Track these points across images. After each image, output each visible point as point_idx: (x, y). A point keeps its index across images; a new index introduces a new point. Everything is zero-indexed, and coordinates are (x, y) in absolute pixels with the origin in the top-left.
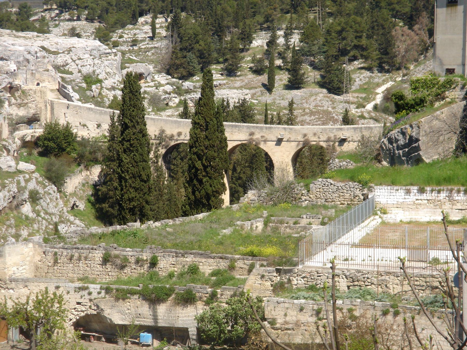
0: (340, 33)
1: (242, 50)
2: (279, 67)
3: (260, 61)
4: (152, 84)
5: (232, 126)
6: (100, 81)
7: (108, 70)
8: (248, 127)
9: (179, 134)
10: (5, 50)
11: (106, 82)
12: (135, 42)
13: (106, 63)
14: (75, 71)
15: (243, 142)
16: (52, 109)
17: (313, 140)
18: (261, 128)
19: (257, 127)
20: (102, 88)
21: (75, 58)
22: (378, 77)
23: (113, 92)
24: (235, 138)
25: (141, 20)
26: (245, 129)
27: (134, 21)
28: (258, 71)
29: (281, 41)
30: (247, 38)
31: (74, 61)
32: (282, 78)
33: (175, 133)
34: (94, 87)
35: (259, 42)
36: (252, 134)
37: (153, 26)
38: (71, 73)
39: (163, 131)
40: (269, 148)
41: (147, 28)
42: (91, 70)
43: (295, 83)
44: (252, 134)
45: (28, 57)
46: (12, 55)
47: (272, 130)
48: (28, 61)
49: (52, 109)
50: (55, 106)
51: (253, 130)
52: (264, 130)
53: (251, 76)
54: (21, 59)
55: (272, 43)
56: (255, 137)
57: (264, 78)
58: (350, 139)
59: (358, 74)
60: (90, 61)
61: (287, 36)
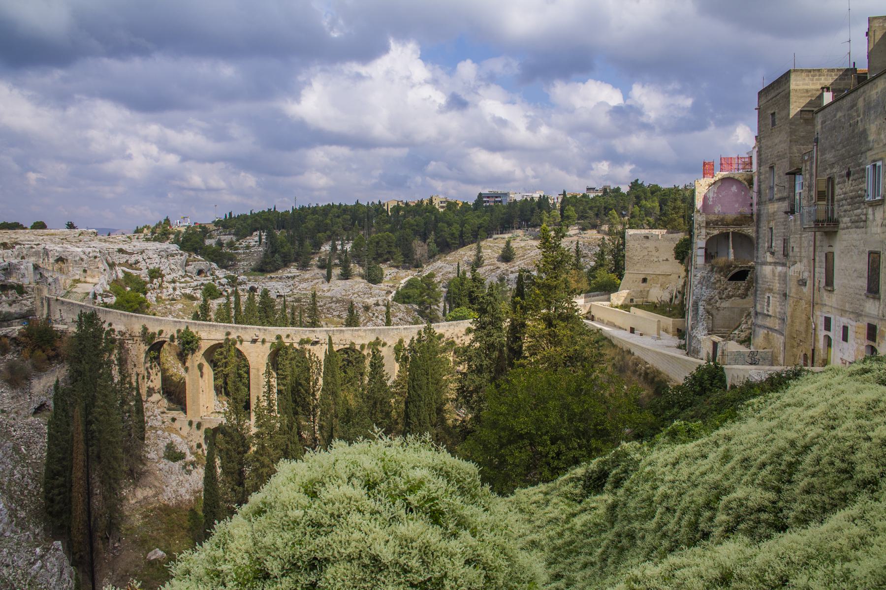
0: (378, 243)
1: (313, 253)
2: (336, 265)
3: (324, 260)
4: (211, 278)
5: (210, 325)
6: (164, 276)
7: (173, 267)
8: (225, 327)
9: (161, 332)
11: (167, 277)
12: (248, 247)
13: (172, 261)
14: (144, 268)
16: (49, 305)
17: (287, 342)
18: (237, 328)
19: (233, 327)
20: (163, 281)
21: (145, 257)
22: (402, 273)
24: (212, 337)
25: (255, 233)
26: (222, 329)
27: (251, 234)
28: (321, 267)
29: (339, 247)
30: (317, 245)
32: (337, 271)
33: (157, 331)
34: (155, 280)
35: (326, 248)
36: (228, 334)
37: (260, 236)
38: (141, 269)
39: (145, 329)
40: (246, 348)
41: (257, 239)
42: (157, 266)
43: (346, 275)
44: (228, 334)
45: (84, 257)
48: (82, 260)
49: (49, 305)
50: (52, 303)
53: (317, 271)
54: (78, 258)
55: (334, 248)
56: (230, 337)
57: (325, 272)
58: (323, 342)
59: (388, 271)
60: (158, 260)
61: (342, 245)
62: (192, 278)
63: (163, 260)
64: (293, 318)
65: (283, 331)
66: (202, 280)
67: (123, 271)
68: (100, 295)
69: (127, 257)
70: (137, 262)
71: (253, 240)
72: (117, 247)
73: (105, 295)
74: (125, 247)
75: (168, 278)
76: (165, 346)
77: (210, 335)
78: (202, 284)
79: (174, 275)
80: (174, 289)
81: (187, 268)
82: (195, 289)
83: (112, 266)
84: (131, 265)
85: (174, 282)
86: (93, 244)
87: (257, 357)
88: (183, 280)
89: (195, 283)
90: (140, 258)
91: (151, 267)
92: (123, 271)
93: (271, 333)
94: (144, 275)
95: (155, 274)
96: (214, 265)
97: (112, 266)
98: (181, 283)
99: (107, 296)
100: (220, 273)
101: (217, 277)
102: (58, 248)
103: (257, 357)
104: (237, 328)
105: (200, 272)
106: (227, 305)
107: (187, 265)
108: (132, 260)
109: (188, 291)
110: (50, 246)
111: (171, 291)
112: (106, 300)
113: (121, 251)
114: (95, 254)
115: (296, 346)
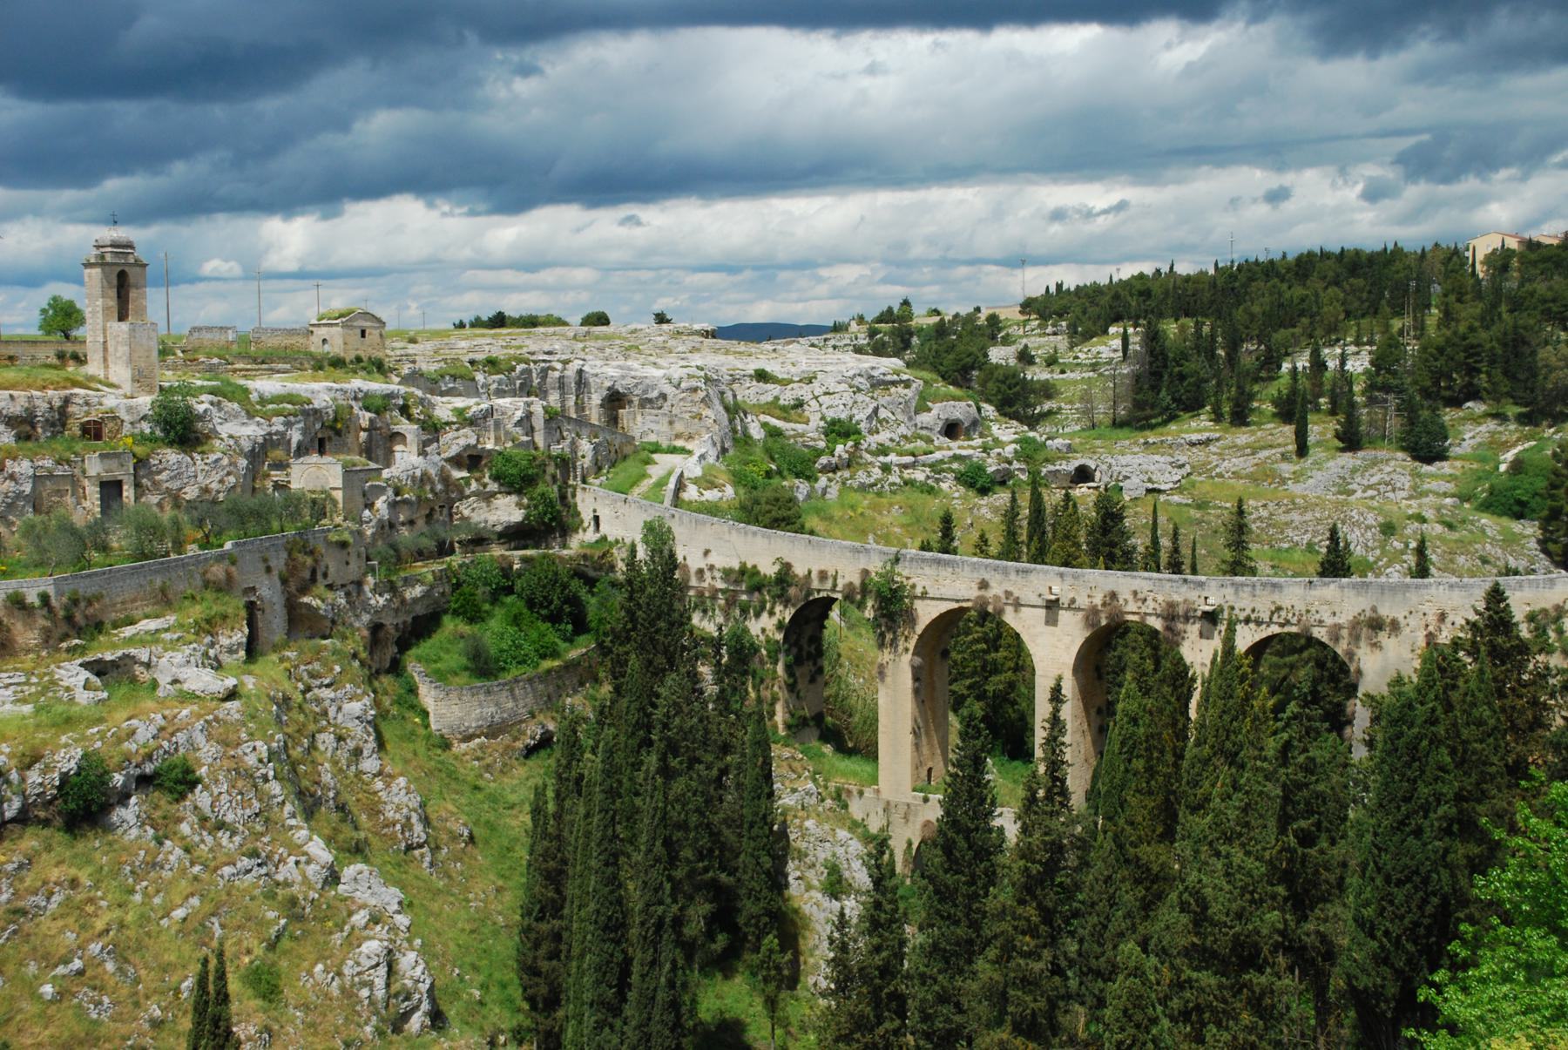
10: (623, 377)
11: (870, 439)
15: (965, 605)
17: (1131, 610)
23: (881, 458)
29: (1332, 364)
31: (816, 398)
36: (984, 585)
40: (1026, 624)
41: (1117, 343)
44: (984, 585)
45: (668, 389)
46: (636, 386)
47: (1032, 577)
48: (664, 396)
51: (987, 577)
52: (1013, 576)
56: (989, 594)
57: (1289, 430)
60: (847, 397)
62: (929, 441)
63: (860, 397)
64: (1176, 550)
65: (1124, 583)
66: (957, 447)
67: (764, 425)
68: (696, 481)
69: (772, 390)
70: (799, 404)
71: (1108, 347)
72: (752, 366)
73: (706, 482)
74: (771, 367)
75: (872, 441)
76: (835, 614)
77: (941, 587)
78: (956, 458)
79: (884, 437)
80: (886, 468)
81: (924, 418)
82: (936, 467)
83: (734, 410)
84: (784, 409)
85: (883, 450)
86: (697, 360)
87: (1053, 651)
88: (908, 446)
89: (938, 455)
90: (804, 392)
91: (830, 415)
92: (764, 425)
93: (1093, 585)
94: (809, 430)
95: (839, 430)
96: (989, 410)
97: (734, 410)
98: (900, 454)
99: (712, 485)
100: (1007, 433)
101: (996, 440)
102: (611, 371)
103: (1053, 651)
104: (1006, 572)
105: (952, 430)
106: (1011, 515)
107: (922, 408)
108: (787, 397)
109: (919, 475)
110: (593, 366)
111: (877, 473)
112: (711, 495)
113: (762, 376)
114: (694, 383)
115: (1156, 623)
